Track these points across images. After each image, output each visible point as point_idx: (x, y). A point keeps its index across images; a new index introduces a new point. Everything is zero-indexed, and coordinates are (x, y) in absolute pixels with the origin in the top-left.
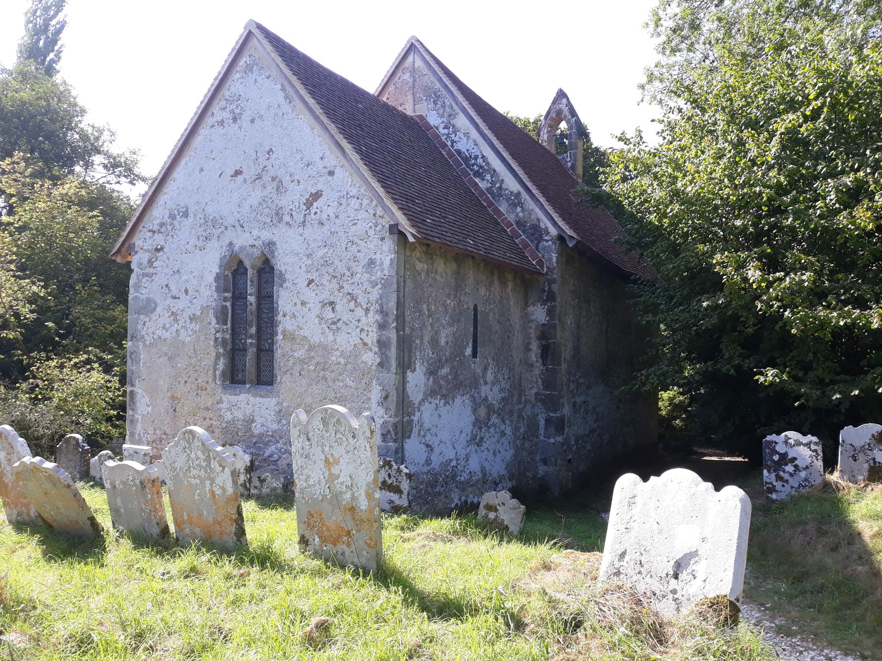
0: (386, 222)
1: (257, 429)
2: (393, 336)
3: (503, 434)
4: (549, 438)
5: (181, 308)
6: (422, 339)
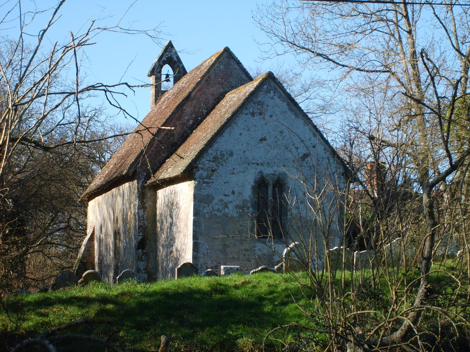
5: (230, 200)
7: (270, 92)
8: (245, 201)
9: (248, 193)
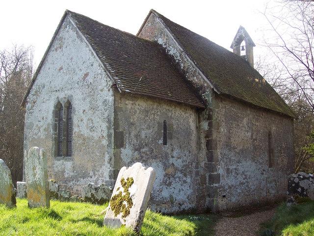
0: (111, 83)
1: (66, 176)
2: (112, 131)
3: (185, 182)
4: (210, 184)
6: (130, 134)
7: (66, 27)
8: (48, 124)
9: (50, 118)
